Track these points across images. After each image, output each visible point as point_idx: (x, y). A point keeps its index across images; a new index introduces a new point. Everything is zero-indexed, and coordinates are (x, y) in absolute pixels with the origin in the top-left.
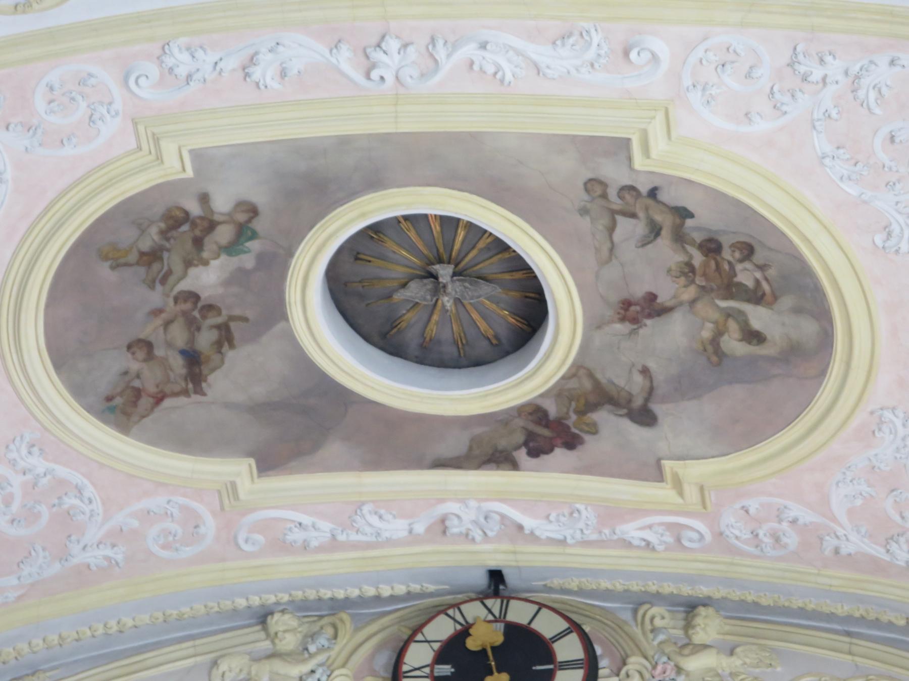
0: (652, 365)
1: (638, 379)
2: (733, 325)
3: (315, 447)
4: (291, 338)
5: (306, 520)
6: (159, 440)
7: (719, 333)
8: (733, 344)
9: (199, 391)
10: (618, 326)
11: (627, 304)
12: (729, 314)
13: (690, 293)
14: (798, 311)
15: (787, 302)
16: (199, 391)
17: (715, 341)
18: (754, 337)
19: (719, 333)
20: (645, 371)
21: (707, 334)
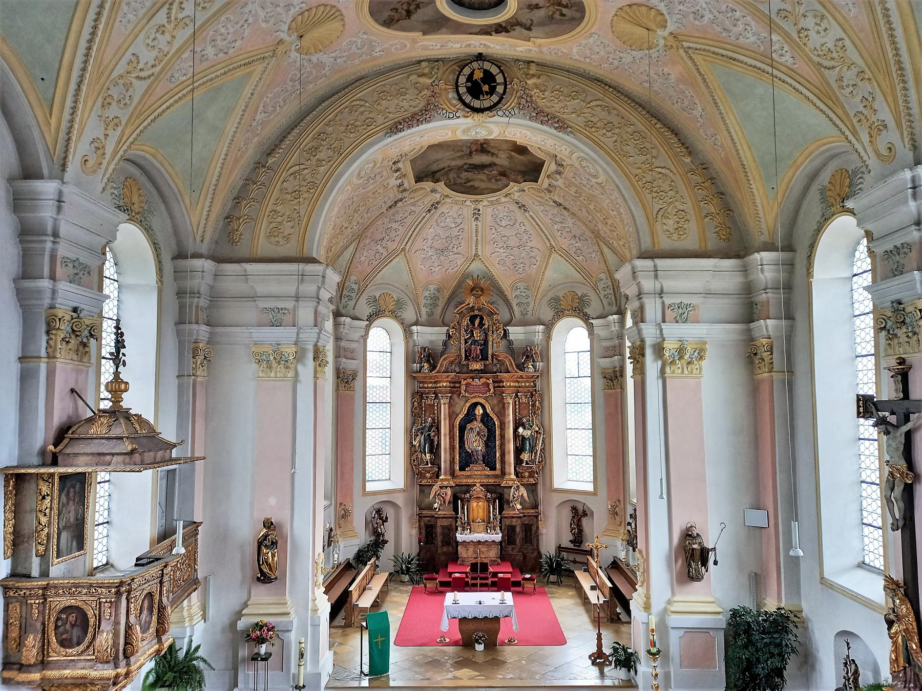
0: (533, 19)
1: (529, 21)
2: (558, 12)
3: (439, 29)
4: (435, 6)
5: (434, 44)
6: (397, 30)
7: (554, 13)
8: (557, 16)
9: (409, 18)
10: (527, 10)
11: (530, 6)
12: (557, 10)
13: (549, 4)
14: (576, 11)
15: (574, 8)
16: (409, 18)
17: (552, 15)
18: (563, 15)
19: (554, 13)
20: (531, 20)
21: (550, 13)
